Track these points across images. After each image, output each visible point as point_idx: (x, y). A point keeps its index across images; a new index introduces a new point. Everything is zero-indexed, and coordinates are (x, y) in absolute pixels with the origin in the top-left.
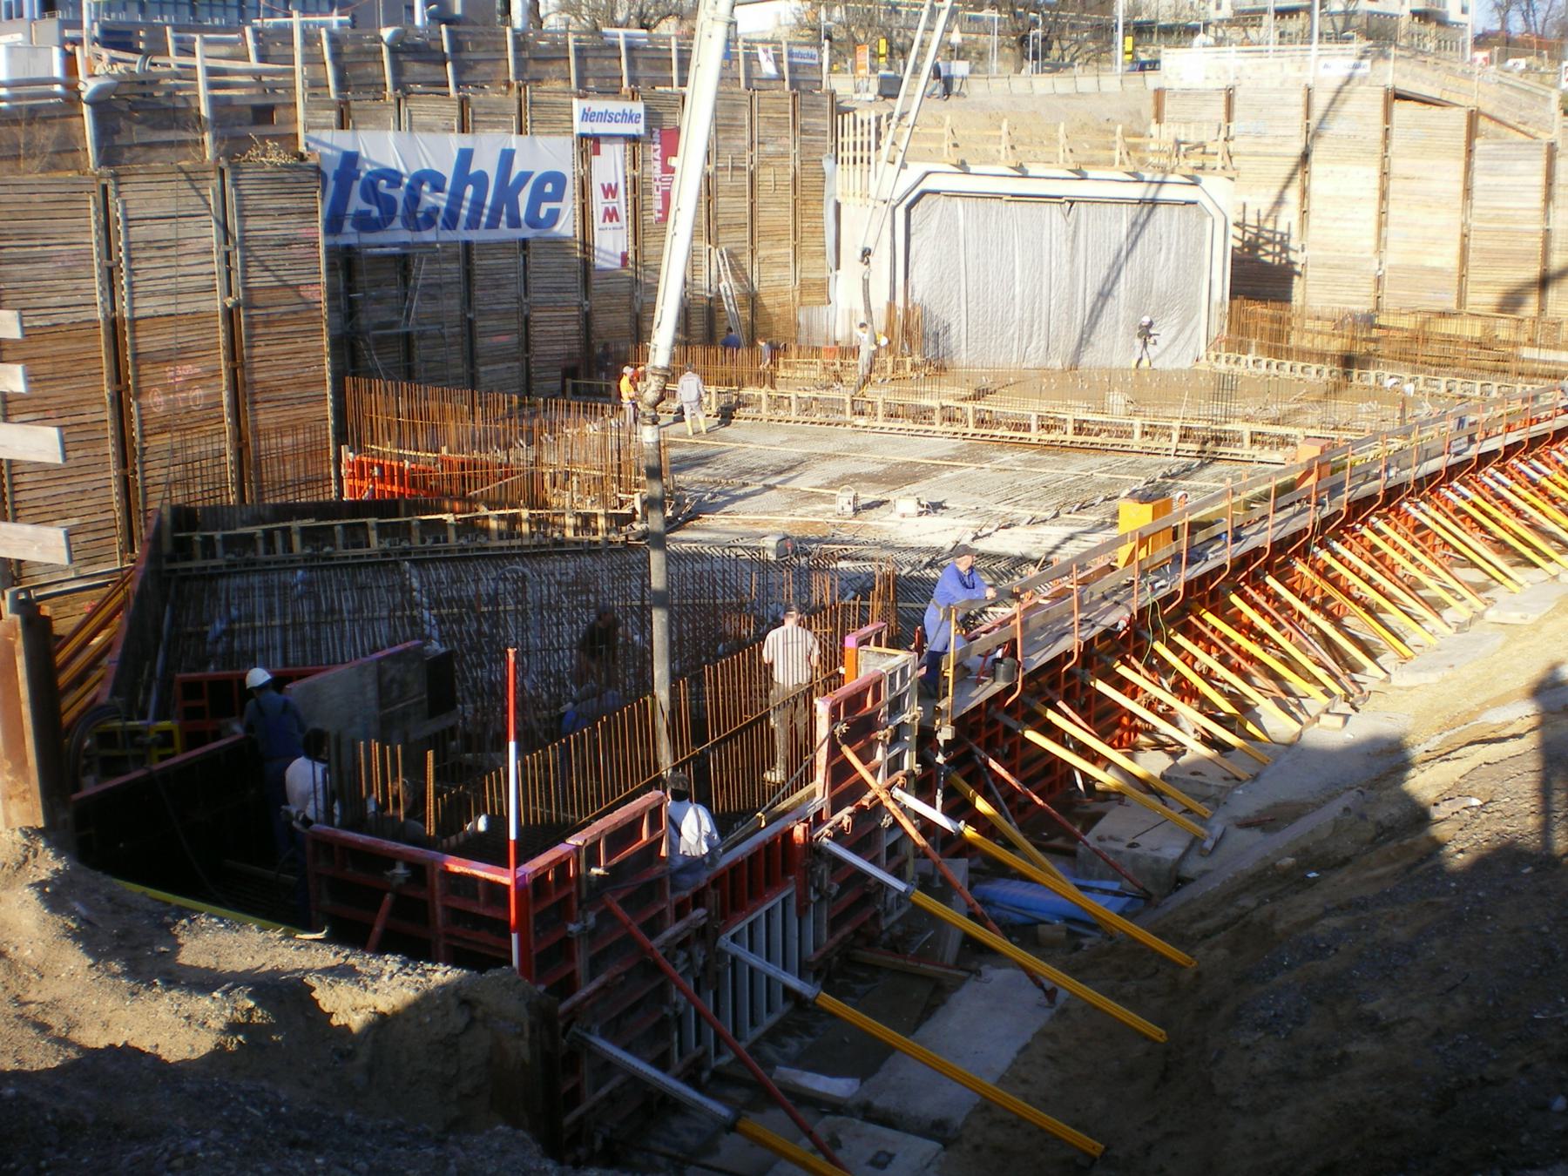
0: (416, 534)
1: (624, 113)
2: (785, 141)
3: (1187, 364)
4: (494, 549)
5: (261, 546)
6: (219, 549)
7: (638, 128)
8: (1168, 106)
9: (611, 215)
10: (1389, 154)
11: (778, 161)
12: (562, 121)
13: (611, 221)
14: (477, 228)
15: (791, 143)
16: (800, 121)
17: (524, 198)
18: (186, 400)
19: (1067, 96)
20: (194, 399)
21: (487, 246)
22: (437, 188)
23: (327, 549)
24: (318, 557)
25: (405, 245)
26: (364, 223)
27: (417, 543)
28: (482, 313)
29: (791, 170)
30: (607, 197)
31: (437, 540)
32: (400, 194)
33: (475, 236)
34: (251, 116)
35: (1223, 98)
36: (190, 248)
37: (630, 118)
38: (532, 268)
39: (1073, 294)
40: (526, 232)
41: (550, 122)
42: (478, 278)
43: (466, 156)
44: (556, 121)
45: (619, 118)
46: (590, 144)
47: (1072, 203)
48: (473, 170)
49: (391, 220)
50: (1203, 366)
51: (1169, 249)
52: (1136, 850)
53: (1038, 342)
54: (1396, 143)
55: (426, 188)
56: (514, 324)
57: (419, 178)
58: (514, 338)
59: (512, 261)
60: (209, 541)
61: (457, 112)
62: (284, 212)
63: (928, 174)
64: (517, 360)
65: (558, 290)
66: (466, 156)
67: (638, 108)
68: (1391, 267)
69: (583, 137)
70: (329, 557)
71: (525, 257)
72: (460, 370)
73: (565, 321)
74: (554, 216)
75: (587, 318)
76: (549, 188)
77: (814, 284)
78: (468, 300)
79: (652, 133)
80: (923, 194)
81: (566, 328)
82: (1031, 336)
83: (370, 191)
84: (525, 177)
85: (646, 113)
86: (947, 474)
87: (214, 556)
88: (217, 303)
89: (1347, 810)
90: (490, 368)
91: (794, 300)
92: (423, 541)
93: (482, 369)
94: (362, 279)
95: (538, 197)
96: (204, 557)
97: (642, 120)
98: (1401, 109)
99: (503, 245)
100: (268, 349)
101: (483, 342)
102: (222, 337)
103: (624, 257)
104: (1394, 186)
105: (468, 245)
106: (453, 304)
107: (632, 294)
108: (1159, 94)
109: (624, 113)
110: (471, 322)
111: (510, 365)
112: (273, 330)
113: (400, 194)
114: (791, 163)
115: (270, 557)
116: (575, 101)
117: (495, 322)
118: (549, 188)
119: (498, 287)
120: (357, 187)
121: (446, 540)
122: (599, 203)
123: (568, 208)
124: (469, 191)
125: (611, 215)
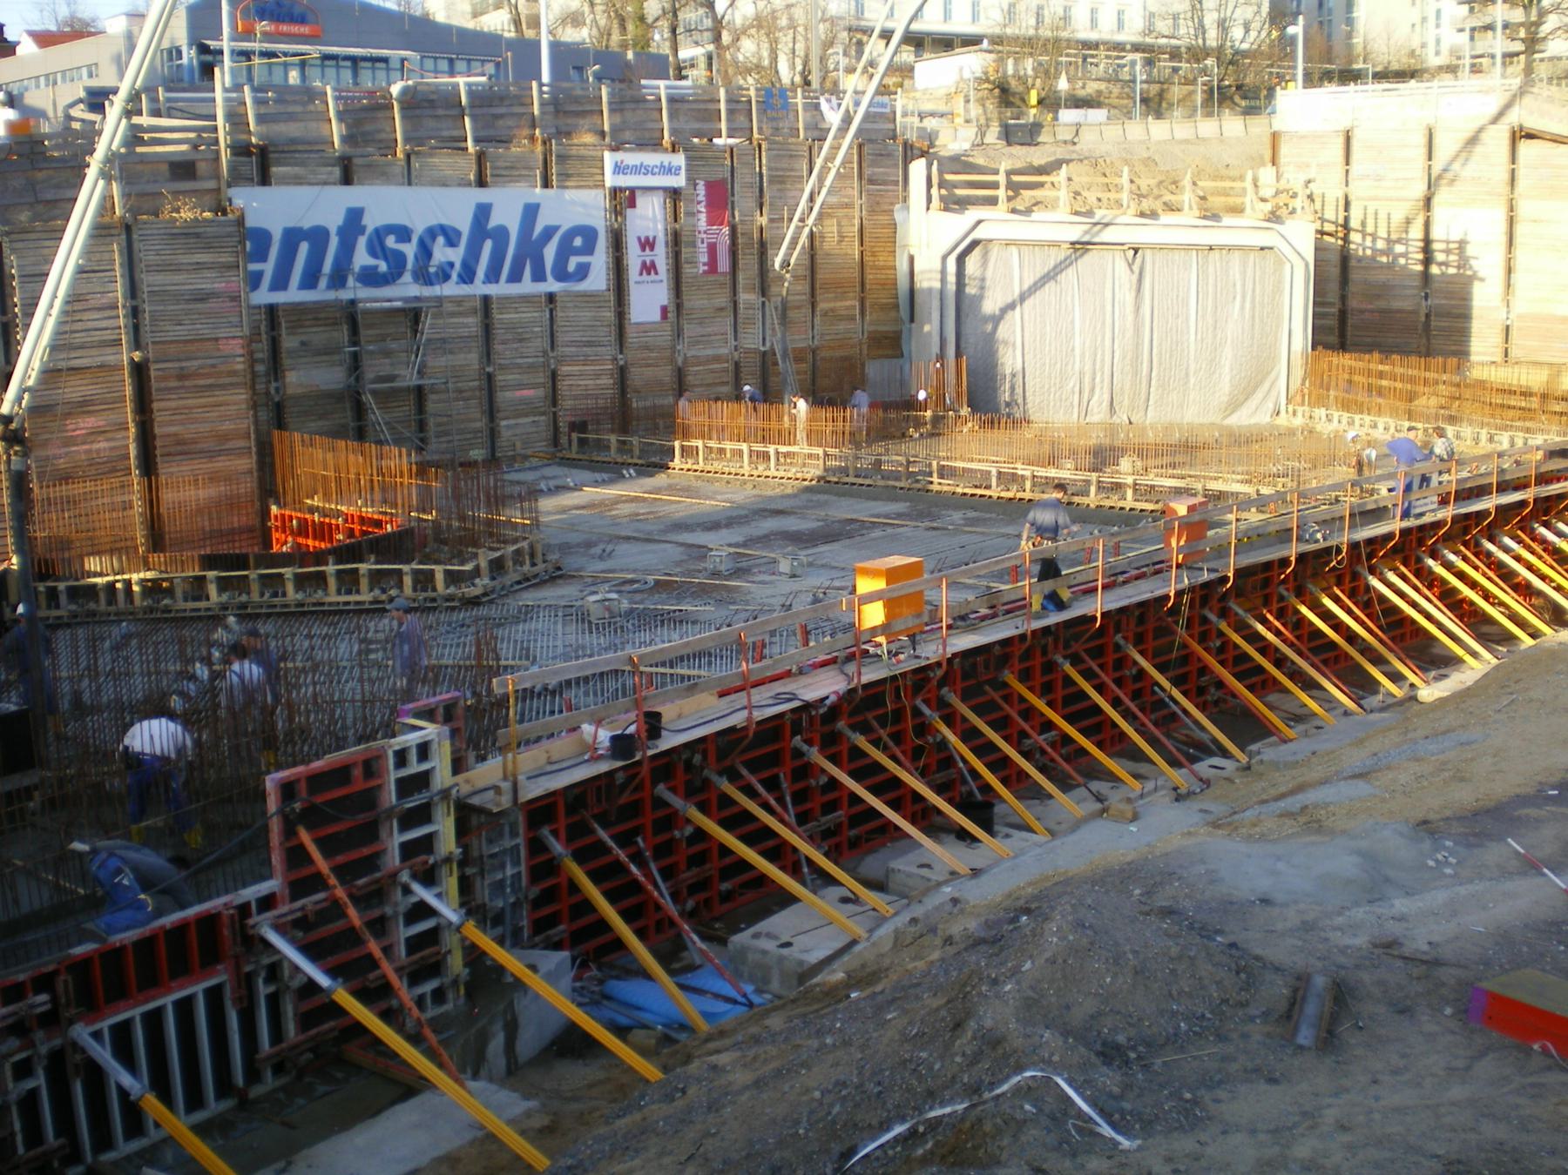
0: (255, 587)
1: (662, 166)
2: (850, 192)
3: (1264, 418)
4: (330, 604)
5: (102, 597)
6: (63, 599)
7: (679, 181)
8: (1285, 150)
9: (649, 268)
10: (1516, 195)
11: (841, 213)
12: (593, 175)
13: (649, 274)
14: (497, 281)
15: (856, 193)
16: (867, 172)
17: (550, 253)
18: (88, 452)
19: (1187, 141)
20: (98, 451)
21: (507, 300)
22: (452, 242)
23: (166, 602)
24: (157, 610)
25: (417, 299)
26: (370, 278)
27: (255, 597)
28: (502, 367)
29: (857, 222)
30: (643, 249)
31: (275, 595)
32: (410, 250)
33: (492, 290)
34: (167, 174)
35: (1341, 140)
36: (92, 303)
37: (670, 170)
38: (559, 322)
39: (1138, 345)
40: (552, 285)
41: (579, 175)
42: (499, 333)
43: (483, 212)
44: (588, 173)
45: (656, 170)
46: (623, 200)
47: (1136, 251)
48: (494, 222)
49: (400, 275)
50: (1283, 420)
51: (1244, 297)
52: (785, 951)
53: (1100, 400)
54: (1521, 183)
55: (441, 240)
56: (541, 378)
57: (432, 233)
58: (540, 392)
59: (536, 318)
60: (53, 594)
61: (474, 167)
62: (199, 267)
63: (979, 222)
64: (543, 414)
65: (590, 344)
66: (483, 212)
67: (679, 159)
68: (1520, 317)
69: (615, 192)
70: (167, 610)
71: (551, 311)
72: (478, 425)
73: (598, 376)
74: (583, 272)
75: (622, 372)
76: (578, 242)
77: (886, 338)
78: (488, 354)
79: (695, 185)
80: (975, 244)
81: (598, 382)
82: (1092, 390)
83: (377, 246)
84: (549, 232)
85: (687, 165)
86: (877, 533)
87: (58, 607)
88: (126, 355)
89: (914, 921)
90: (512, 422)
91: (861, 354)
92: (262, 595)
93: (503, 423)
94: (364, 333)
95: (565, 251)
96: (49, 607)
98: (1525, 147)
99: (526, 299)
100: (181, 403)
101: (504, 397)
102: (128, 390)
103: (664, 310)
104: (1520, 230)
105: (486, 300)
106: (471, 359)
107: (673, 348)
108: (1275, 138)
109: (662, 166)
110: (490, 377)
111: (536, 419)
112: (187, 383)
113: (410, 250)
114: (857, 214)
115: (112, 609)
116: (607, 155)
117: (517, 376)
118: (578, 242)
119: (521, 341)
120: (362, 242)
121: (284, 595)
122: (634, 258)
123: (600, 261)
124: (488, 246)
125: (649, 268)
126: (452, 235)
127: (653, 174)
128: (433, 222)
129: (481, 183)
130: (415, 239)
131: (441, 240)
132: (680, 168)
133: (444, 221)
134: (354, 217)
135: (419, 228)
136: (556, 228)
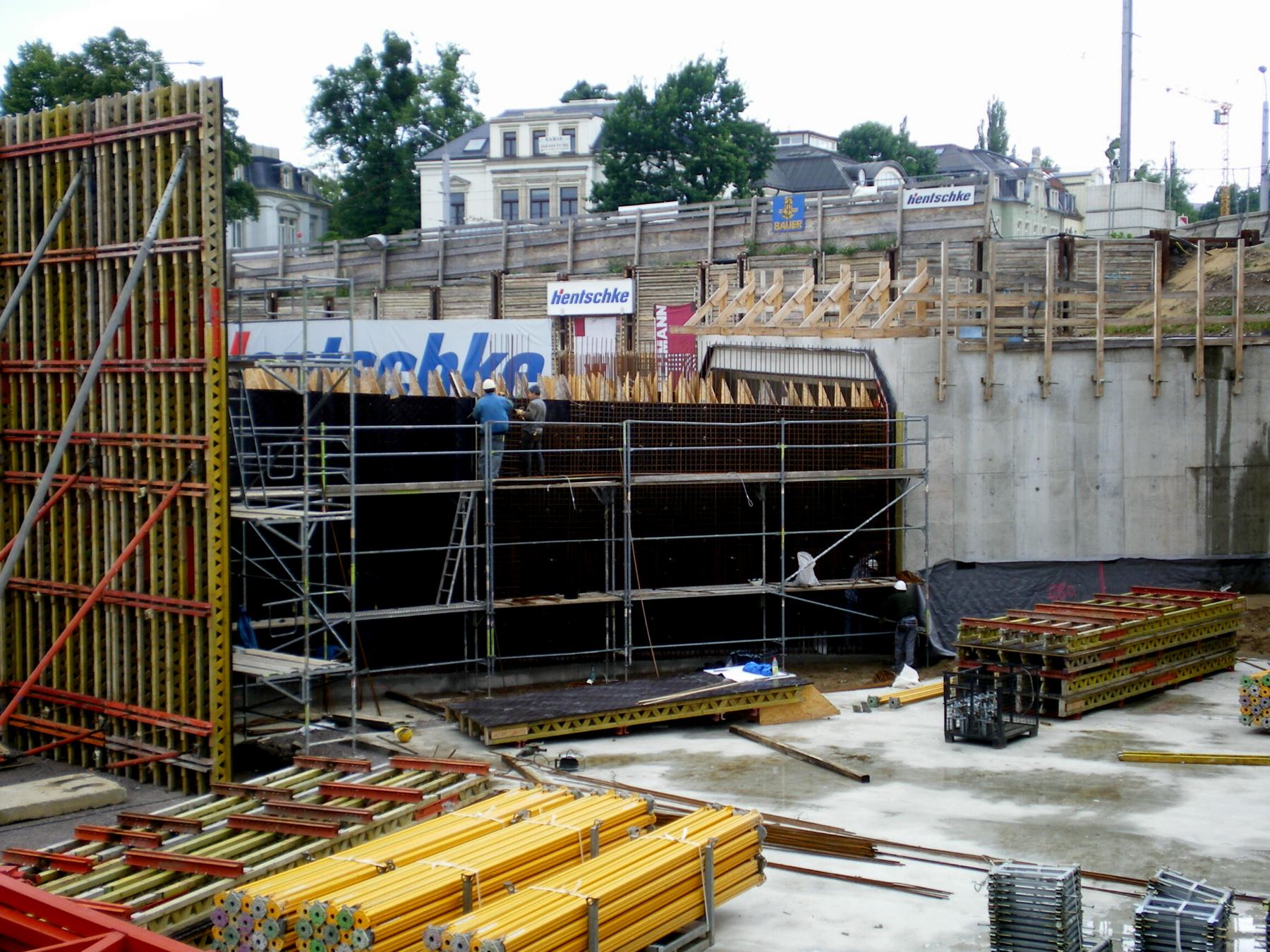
7: (628, 308)
22: (408, 366)
37: (615, 297)
41: (528, 306)
43: (435, 341)
46: (567, 327)
48: (444, 350)
55: (399, 365)
57: (392, 359)
66: (435, 341)
67: (626, 285)
69: (562, 321)
76: (524, 368)
84: (496, 359)
85: (636, 290)
97: (630, 299)
118: (524, 368)
126: (408, 359)
127: (595, 302)
128: (393, 349)
129: (435, 315)
130: (377, 365)
131: (399, 365)
132: (628, 294)
133: (403, 349)
134: (333, 344)
135: (381, 354)
136: (504, 355)
